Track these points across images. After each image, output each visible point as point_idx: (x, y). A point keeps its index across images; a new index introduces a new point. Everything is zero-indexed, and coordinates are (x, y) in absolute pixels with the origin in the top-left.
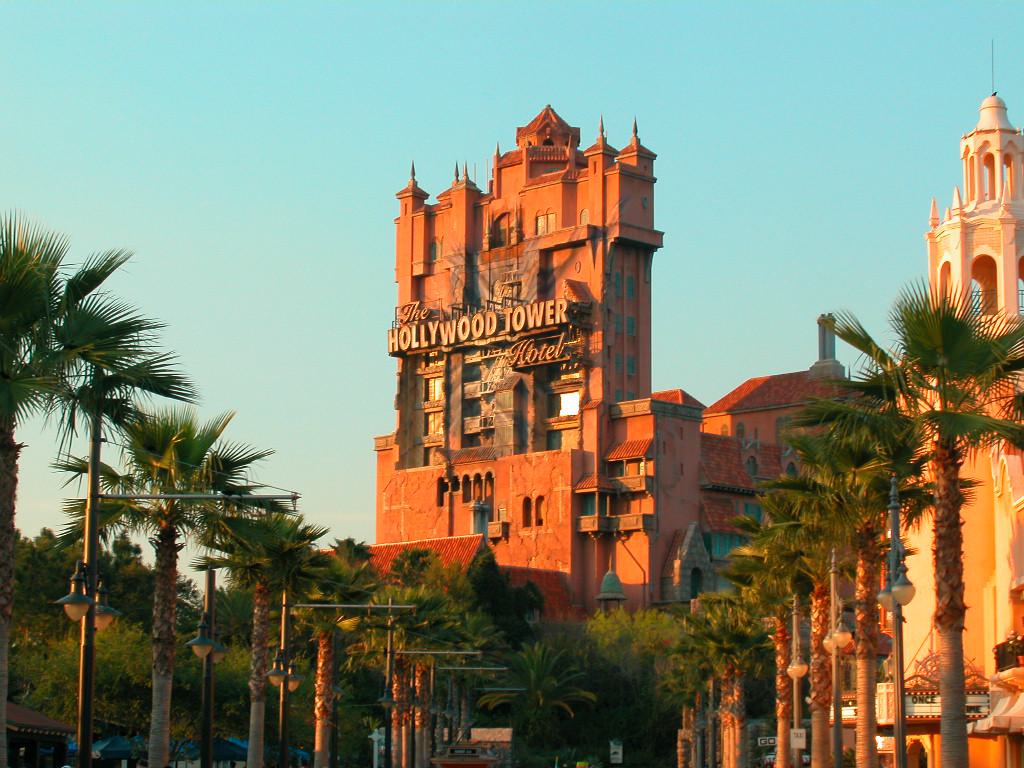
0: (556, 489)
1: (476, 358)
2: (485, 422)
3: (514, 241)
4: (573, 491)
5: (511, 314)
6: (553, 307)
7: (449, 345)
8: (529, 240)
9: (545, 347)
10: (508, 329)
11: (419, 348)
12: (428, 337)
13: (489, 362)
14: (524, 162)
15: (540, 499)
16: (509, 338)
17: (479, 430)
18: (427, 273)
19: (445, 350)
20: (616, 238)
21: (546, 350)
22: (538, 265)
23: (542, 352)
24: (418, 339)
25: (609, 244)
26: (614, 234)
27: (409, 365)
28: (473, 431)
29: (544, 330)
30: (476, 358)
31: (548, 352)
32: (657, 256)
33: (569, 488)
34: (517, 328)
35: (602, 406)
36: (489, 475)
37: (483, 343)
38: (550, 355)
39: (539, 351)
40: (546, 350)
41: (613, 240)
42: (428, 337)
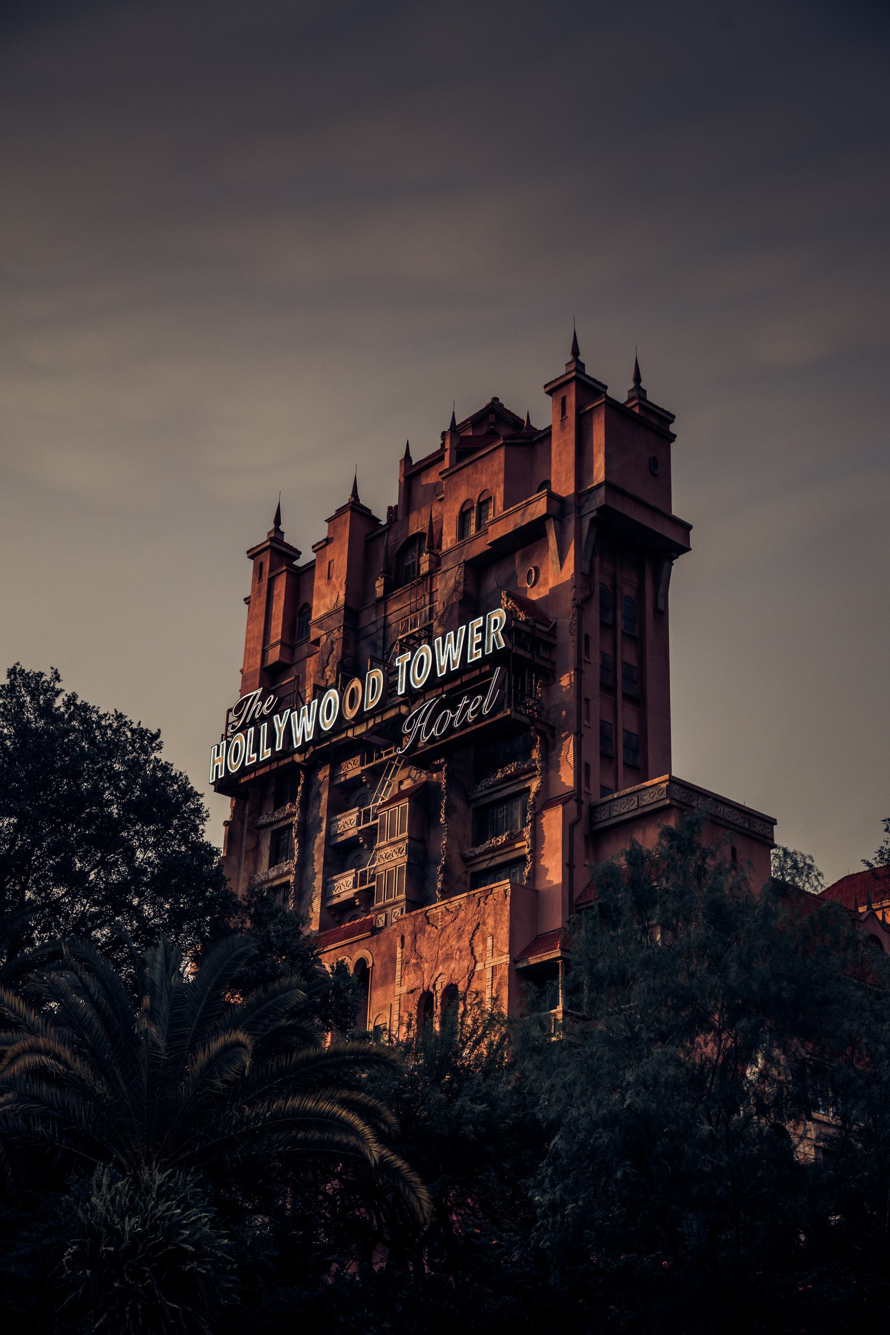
0: (479, 967)
1: (352, 769)
2: (362, 879)
3: (425, 568)
4: (514, 961)
5: (409, 663)
6: (481, 630)
7: (305, 746)
8: (449, 551)
9: (465, 701)
10: (401, 691)
11: (258, 765)
12: (271, 743)
13: (376, 774)
14: (447, 455)
15: (451, 991)
16: (404, 709)
17: (350, 894)
18: (287, 661)
19: (298, 758)
20: (599, 510)
21: (467, 707)
22: (461, 588)
23: (458, 713)
24: (256, 749)
25: (586, 524)
26: (600, 498)
27: (247, 807)
28: (344, 897)
29: (465, 678)
30: (352, 769)
31: (470, 710)
32: (680, 567)
33: (506, 959)
34: (419, 682)
35: (572, 804)
36: (362, 962)
37: (360, 730)
38: (473, 713)
39: (454, 712)
40: (467, 707)
41: (594, 514)
42: (271, 743)
